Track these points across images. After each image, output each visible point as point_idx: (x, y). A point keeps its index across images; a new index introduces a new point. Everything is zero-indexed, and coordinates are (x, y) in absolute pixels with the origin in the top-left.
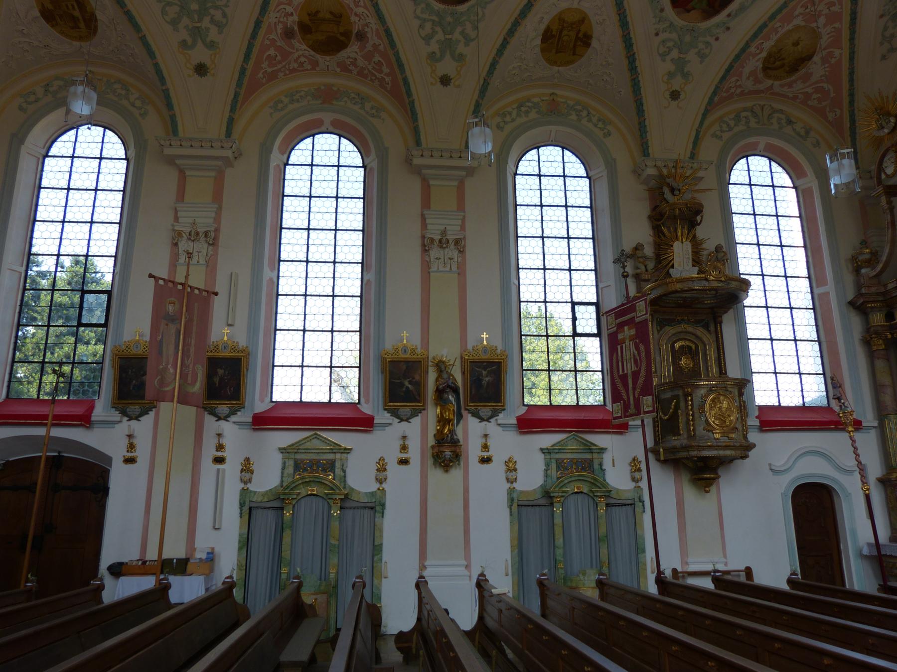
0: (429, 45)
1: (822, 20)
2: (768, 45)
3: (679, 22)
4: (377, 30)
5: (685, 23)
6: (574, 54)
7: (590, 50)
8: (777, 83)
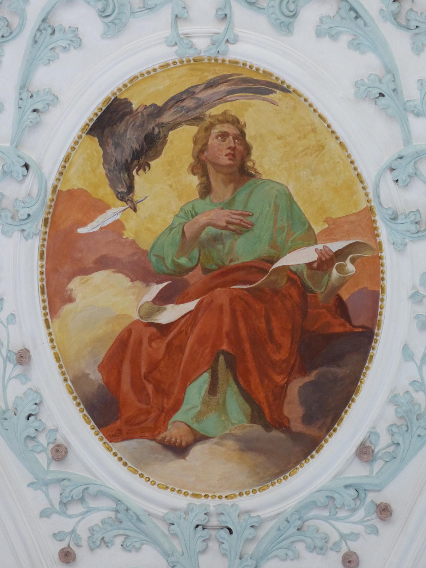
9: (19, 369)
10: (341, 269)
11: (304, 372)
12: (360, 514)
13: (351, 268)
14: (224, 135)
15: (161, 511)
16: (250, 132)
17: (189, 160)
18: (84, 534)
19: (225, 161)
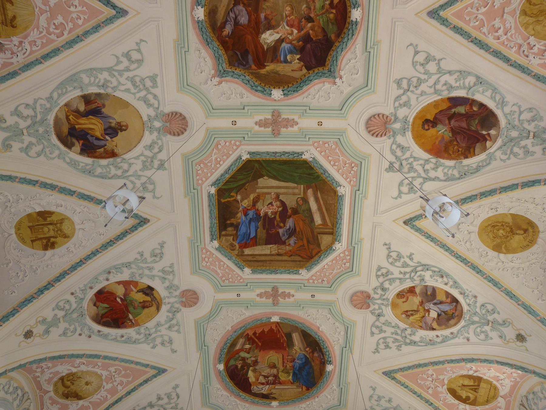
0: (11, 115)
1: (109, 386)
2: (83, 368)
3: (85, 304)
4: (12, 63)
5: (86, 308)
6: (32, 241)
7: (41, 252)
8: (52, 394)
9: (105, 279)
11: (111, 320)
12: (89, 333)
13: (130, 323)
15: (83, 305)
16: (151, 308)
17: (145, 300)
18: (76, 295)
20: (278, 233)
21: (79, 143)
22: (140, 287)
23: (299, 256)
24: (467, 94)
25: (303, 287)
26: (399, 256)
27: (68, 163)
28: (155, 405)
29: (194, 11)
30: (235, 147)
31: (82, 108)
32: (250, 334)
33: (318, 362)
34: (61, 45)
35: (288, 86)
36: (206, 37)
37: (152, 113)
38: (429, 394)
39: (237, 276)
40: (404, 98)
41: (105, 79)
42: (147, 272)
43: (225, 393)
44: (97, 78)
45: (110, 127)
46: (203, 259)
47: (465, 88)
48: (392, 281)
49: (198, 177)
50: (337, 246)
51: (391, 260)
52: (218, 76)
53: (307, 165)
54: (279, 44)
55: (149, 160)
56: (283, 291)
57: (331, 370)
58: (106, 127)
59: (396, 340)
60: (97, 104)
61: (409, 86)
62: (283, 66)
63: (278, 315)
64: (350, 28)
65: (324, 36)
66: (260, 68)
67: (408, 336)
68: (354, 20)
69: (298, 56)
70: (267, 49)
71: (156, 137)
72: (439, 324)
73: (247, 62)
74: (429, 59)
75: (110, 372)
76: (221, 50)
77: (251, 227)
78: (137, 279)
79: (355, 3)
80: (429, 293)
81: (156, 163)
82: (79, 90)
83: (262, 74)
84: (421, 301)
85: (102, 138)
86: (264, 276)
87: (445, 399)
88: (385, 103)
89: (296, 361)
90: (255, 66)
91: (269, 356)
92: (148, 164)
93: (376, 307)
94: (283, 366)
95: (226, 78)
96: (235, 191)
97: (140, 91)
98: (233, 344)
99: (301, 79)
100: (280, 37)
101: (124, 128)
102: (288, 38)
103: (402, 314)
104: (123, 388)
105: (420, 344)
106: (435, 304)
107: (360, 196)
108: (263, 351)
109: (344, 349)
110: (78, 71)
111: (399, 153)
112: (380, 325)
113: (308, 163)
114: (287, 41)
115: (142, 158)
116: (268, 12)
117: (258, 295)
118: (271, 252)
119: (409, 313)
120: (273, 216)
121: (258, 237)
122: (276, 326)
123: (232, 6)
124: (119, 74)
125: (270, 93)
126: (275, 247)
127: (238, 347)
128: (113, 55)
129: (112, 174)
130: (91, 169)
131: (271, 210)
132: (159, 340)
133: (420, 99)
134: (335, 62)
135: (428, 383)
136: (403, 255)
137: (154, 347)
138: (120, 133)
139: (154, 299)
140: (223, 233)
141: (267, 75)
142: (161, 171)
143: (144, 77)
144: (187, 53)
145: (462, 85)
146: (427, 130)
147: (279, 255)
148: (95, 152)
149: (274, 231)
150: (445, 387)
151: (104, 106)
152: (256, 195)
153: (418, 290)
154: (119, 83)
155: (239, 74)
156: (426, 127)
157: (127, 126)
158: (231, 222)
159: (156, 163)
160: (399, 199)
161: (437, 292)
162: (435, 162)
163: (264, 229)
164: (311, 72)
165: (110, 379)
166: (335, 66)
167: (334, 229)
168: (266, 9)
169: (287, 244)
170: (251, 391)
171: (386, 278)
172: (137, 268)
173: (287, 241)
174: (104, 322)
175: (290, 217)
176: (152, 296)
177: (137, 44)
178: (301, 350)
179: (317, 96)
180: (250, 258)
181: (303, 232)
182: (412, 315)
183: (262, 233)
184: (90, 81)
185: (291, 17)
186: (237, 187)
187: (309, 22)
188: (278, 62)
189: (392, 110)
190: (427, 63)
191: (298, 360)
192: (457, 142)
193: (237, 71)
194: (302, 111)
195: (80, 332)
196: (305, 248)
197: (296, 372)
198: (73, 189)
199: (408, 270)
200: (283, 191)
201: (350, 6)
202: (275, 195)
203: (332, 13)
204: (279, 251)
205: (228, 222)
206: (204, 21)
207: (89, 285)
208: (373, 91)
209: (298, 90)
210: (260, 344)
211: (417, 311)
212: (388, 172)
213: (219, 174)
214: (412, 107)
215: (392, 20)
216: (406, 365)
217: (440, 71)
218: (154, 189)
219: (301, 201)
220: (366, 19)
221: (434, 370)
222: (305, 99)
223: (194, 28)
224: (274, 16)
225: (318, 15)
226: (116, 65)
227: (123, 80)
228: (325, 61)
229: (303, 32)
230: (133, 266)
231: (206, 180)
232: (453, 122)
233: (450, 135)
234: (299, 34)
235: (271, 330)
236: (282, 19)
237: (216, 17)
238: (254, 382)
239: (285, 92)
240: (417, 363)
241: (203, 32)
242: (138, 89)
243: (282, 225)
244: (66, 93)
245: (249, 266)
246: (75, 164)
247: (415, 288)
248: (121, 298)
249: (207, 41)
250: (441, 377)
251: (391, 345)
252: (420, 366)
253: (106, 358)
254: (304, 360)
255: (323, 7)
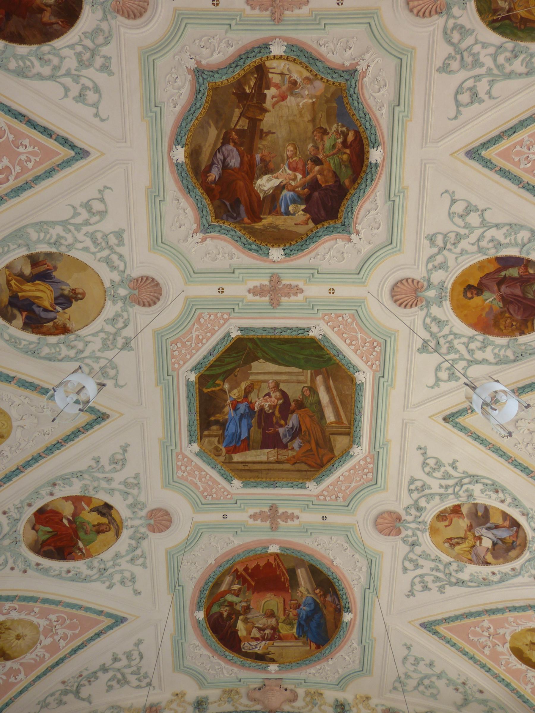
1: (49, 641)
2: (15, 615)
3: (21, 526)
5: (21, 532)
10: (79, 552)
11: (55, 549)
12: (23, 567)
13: (79, 554)
14: (106, 528)
15: (18, 529)
16: (107, 533)
17: (101, 522)
18: (10, 514)
19: (101, 529)
20: (278, 433)
21: (22, 315)
22: (94, 505)
23: (306, 463)
24: (520, 252)
25: (311, 506)
26: (439, 464)
27: (7, 341)
28: (110, 669)
29: (172, 151)
30: (222, 322)
31: (27, 271)
32: (239, 570)
33: (331, 609)
34: (4, 193)
35: (291, 244)
36: (187, 183)
37: (117, 278)
38: (486, 655)
39: (222, 490)
40: (440, 259)
41: (58, 235)
42: (104, 484)
43: (206, 652)
44: (48, 233)
45: (62, 296)
46: (179, 468)
47: (517, 245)
48: (430, 497)
49: (174, 360)
50: (355, 450)
51: (427, 469)
52: (201, 231)
53: (316, 345)
54: (279, 192)
55: (111, 337)
56: (284, 511)
57: (349, 620)
58: (58, 294)
59: (437, 579)
60: (46, 265)
61: (445, 243)
62: (285, 219)
63: (277, 544)
64: (368, 171)
65: (336, 182)
66: (255, 222)
67: (454, 574)
68: (374, 162)
69: (303, 207)
70: (264, 198)
71: (121, 308)
72: (495, 557)
73: (239, 214)
74: (469, 209)
75: (51, 620)
76: (206, 199)
77: (242, 425)
78: (91, 493)
79: (374, 142)
80: (480, 514)
81: (120, 342)
82: (25, 249)
83: (257, 229)
84: (469, 525)
85: (51, 309)
86: (259, 491)
87: (508, 663)
88: (415, 265)
89: (302, 607)
90: (249, 219)
91: (266, 600)
92: (109, 343)
93: (410, 533)
94: (285, 614)
95: (212, 234)
96: (221, 378)
97: (102, 249)
98: (217, 584)
99: (307, 235)
100: (280, 184)
101: (79, 296)
102: (290, 184)
103: (444, 542)
104: (67, 644)
105: (470, 584)
106: (489, 529)
107: (386, 384)
108: (258, 593)
109: (367, 591)
110: (24, 225)
111: (434, 328)
112: (415, 557)
113: (316, 342)
114: (289, 188)
115: (102, 335)
116: (265, 153)
117: (251, 517)
118: (268, 458)
119: (454, 541)
120: (271, 411)
121: (252, 438)
122: (275, 559)
123: (219, 145)
124: (75, 229)
125: (267, 252)
126: (273, 452)
127: (224, 587)
128: (68, 205)
129: (63, 355)
130: (36, 348)
131: (269, 403)
132: (117, 578)
133: (460, 259)
134: (350, 213)
135: (483, 639)
136: (444, 462)
137: (110, 587)
138: (74, 303)
139: (112, 521)
140: (206, 433)
141: (264, 231)
142: (126, 351)
143: (107, 232)
144: (162, 203)
145: (513, 241)
146: (470, 298)
147: (278, 462)
148: (42, 327)
149: (272, 430)
150: (508, 645)
151: (55, 268)
152: (248, 383)
153: (464, 510)
154: (76, 240)
155: (228, 229)
156: (469, 295)
157: (84, 294)
158: (216, 418)
159: (120, 342)
160: (436, 388)
161: (490, 512)
162: (482, 340)
163: (259, 428)
164: (319, 226)
165: (50, 630)
166: (351, 219)
167: (352, 427)
168: (262, 149)
169: (289, 448)
170: (240, 648)
171: (421, 494)
172: (90, 479)
173: (289, 444)
174: (44, 552)
175: (293, 412)
176: (109, 517)
177: (100, 191)
178: (309, 593)
179: (328, 257)
180: (241, 467)
181: (311, 432)
182: (458, 544)
183: (257, 434)
184: (39, 236)
185: (294, 159)
186: (225, 372)
187: (317, 165)
188: (278, 213)
189: (424, 274)
190: (468, 214)
191: (304, 606)
192: (510, 314)
193: (226, 226)
194: (308, 275)
195: (13, 565)
196: (313, 453)
197: (302, 622)
198: (12, 374)
199: (451, 482)
200: (284, 377)
201: (368, 145)
202: (273, 383)
203: (345, 153)
204: (280, 457)
205: (212, 419)
206: (184, 164)
207: (28, 501)
208: (400, 250)
209: (303, 248)
210: (253, 584)
211: (464, 539)
212: (421, 353)
213: (201, 356)
214: (450, 270)
215: (422, 161)
216: (452, 614)
217: (484, 224)
218: (117, 375)
219: (308, 392)
220: (388, 160)
221: (490, 621)
222: (312, 260)
223: (172, 172)
224: (273, 158)
225: (327, 156)
226: (72, 218)
227: (80, 236)
228: (337, 212)
229: (308, 177)
230: (86, 476)
231: (184, 363)
232: (503, 288)
233: (501, 304)
234: (304, 179)
235: (269, 564)
236: (283, 161)
237: (200, 158)
238: (244, 637)
239: (287, 251)
240: (466, 611)
241: (182, 177)
242: (99, 247)
243: (282, 422)
244: (8, 252)
245: (240, 478)
246: (16, 342)
247: (460, 508)
248: (69, 520)
249: (188, 188)
250: (501, 631)
251: (430, 585)
252: (471, 615)
253: (46, 601)
254: (312, 606)
255: (334, 146)
